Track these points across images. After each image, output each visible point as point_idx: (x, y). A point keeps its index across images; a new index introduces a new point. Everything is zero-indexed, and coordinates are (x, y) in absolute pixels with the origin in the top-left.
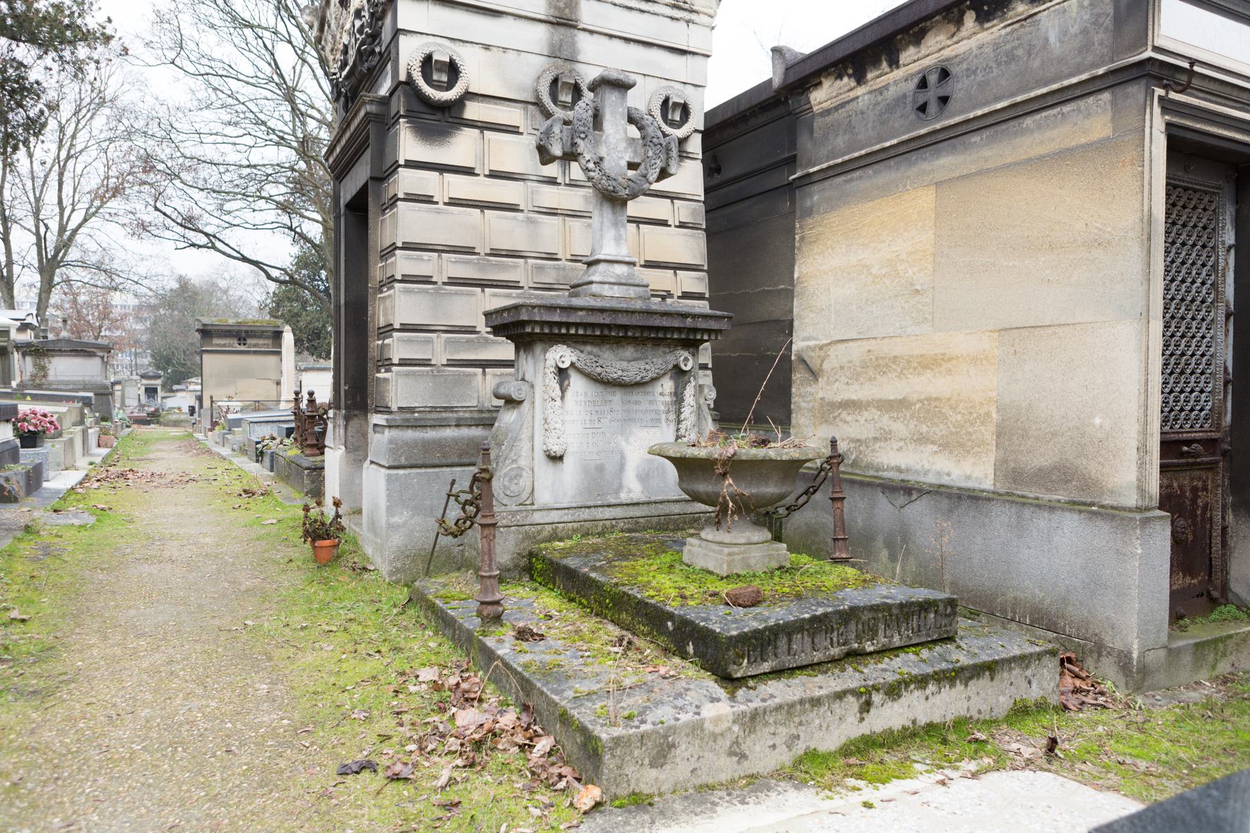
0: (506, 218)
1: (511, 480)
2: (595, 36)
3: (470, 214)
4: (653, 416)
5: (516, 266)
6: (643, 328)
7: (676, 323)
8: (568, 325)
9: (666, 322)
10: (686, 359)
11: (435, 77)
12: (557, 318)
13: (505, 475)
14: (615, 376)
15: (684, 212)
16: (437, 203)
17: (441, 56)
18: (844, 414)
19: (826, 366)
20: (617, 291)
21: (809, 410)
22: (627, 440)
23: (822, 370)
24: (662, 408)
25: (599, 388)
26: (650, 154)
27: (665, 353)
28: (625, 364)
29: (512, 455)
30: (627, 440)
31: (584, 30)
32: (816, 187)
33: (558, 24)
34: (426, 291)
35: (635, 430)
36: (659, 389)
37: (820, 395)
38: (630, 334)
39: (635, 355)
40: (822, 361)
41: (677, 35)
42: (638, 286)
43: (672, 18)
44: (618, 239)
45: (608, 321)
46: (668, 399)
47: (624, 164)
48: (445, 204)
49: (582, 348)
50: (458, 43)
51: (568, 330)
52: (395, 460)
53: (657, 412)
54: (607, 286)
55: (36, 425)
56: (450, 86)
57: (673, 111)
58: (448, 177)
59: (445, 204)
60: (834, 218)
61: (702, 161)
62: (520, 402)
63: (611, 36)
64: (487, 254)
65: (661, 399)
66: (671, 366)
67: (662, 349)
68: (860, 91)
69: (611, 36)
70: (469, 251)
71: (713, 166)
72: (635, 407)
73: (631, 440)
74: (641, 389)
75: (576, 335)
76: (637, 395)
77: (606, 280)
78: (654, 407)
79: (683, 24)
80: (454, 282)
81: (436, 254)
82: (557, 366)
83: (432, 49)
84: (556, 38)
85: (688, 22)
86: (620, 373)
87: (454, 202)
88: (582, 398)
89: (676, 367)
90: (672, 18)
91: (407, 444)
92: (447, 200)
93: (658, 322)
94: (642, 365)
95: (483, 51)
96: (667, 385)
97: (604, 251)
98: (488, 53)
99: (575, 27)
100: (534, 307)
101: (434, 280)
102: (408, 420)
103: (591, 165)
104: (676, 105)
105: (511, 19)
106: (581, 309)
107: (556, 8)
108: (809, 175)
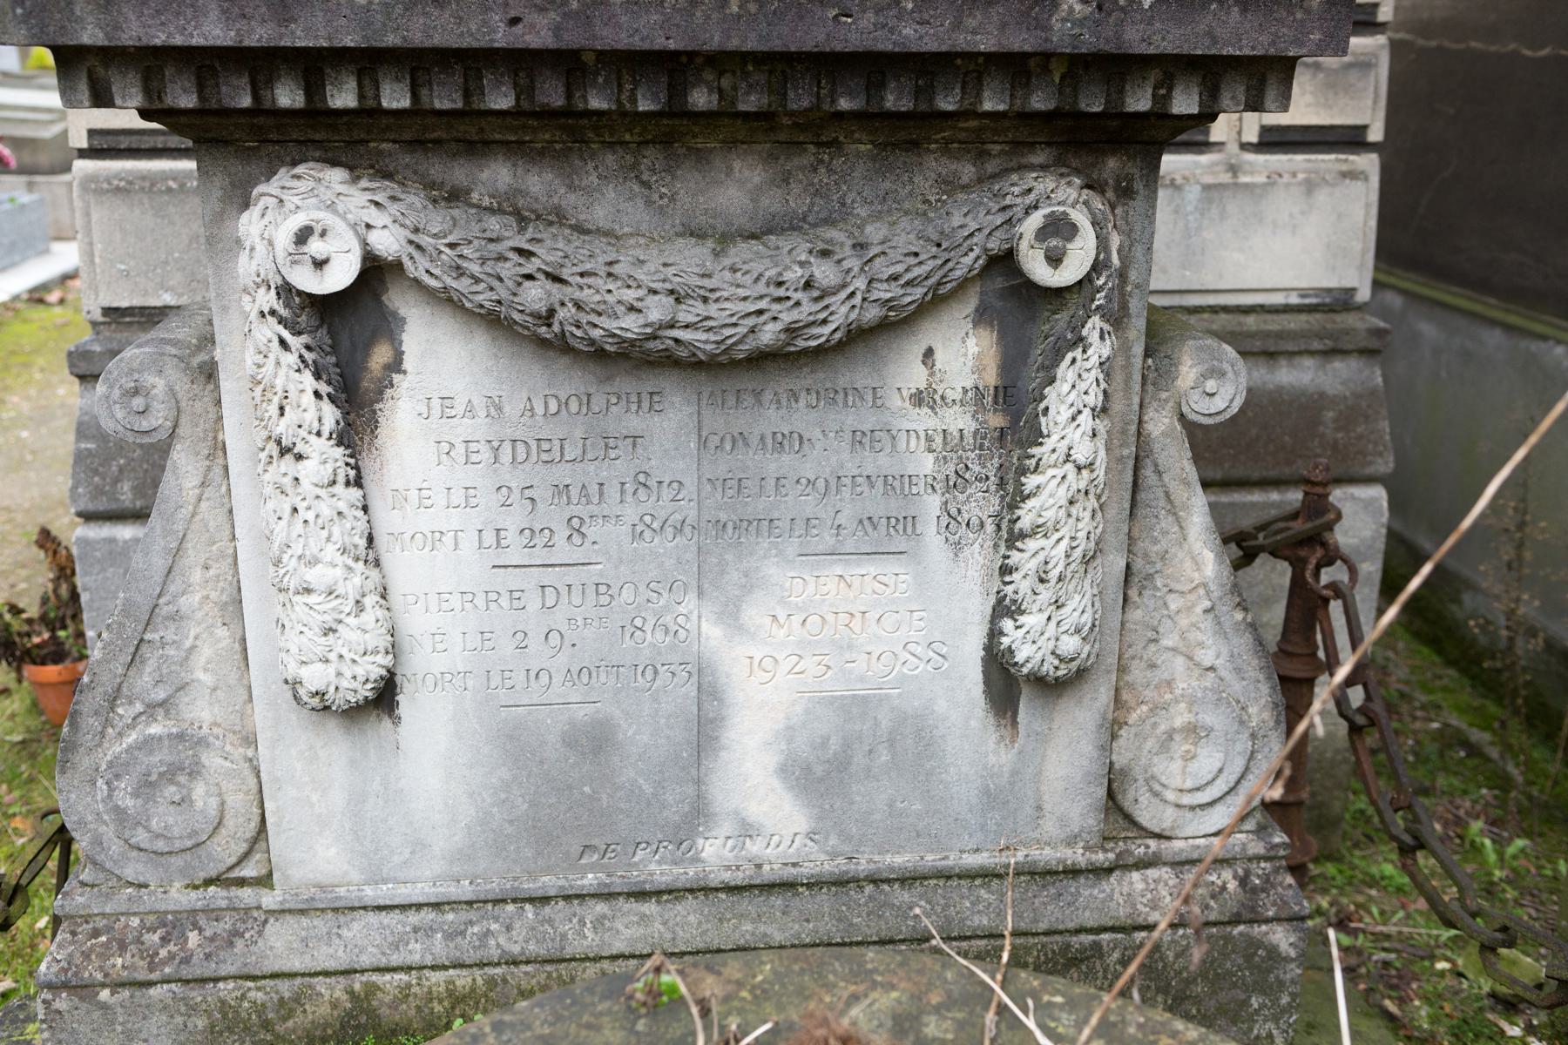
1: (147, 787)
4: (876, 503)
10: (1059, 229)
13: (117, 769)
14: (631, 325)
22: (730, 615)
25: (572, 382)
27: (950, 186)
28: (689, 260)
29: (144, 679)
30: (730, 615)
35: (772, 570)
38: (701, 99)
39: (772, 202)
46: (960, 421)
49: (459, 173)
51: (314, 89)
52: (98, 492)
53: (897, 484)
65: (923, 420)
66: (968, 262)
67: (935, 165)
72: (774, 465)
73: (754, 614)
74: (804, 379)
75: (369, 114)
76: (778, 411)
78: (879, 463)
82: (286, 290)
86: (657, 310)
88: (477, 428)
89: (1004, 262)
94: (793, 260)
96: (962, 352)
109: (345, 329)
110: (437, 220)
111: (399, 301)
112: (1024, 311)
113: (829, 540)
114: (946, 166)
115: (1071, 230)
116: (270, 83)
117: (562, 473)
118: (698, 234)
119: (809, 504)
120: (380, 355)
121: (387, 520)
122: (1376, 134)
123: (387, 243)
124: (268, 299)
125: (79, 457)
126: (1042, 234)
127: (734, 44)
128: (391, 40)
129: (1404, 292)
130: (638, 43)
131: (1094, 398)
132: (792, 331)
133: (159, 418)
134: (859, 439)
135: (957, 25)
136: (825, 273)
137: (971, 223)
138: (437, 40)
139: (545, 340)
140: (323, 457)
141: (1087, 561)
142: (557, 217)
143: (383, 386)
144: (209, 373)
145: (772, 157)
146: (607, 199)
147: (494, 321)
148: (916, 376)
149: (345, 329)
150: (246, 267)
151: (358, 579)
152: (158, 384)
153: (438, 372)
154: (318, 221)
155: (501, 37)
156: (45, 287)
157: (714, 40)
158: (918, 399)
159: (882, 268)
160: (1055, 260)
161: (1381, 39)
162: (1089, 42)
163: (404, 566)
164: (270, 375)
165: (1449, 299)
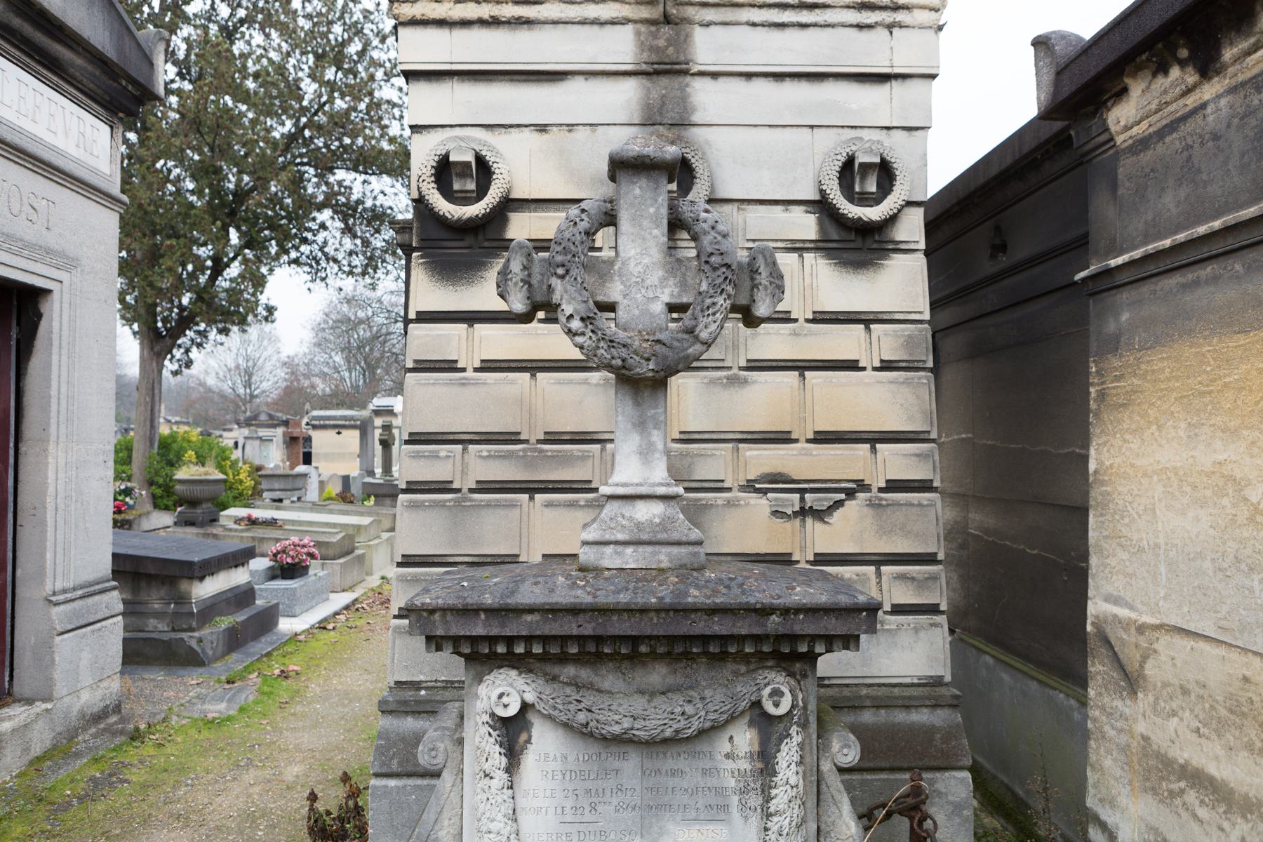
0: (571, 382)
2: (721, 80)
3: (512, 382)
5: (584, 457)
6: (672, 639)
7: (743, 627)
8: (510, 641)
9: (718, 627)
10: (777, 693)
11: (456, 187)
12: (479, 630)
14: (617, 729)
15: (887, 342)
16: (464, 370)
18: (1191, 797)
19: (1150, 670)
20: (631, 558)
21: (1125, 749)
23: (1144, 677)
24: (732, 783)
25: (594, 748)
26: (704, 287)
27: (737, 674)
28: (639, 704)
31: (702, 74)
32: (1124, 296)
33: (658, 73)
34: (441, 504)
35: (671, 826)
36: (726, 747)
37: (1141, 727)
39: (670, 680)
40: (1144, 659)
41: (873, 51)
42: (678, 543)
43: (860, 27)
44: (645, 453)
45: (588, 630)
46: (745, 765)
47: (658, 308)
48: (476, 370)
52: (383, 764)
53: (720, 791)
54: (609, 550)
55: (293, 558)
56: (482, 192)
58: (481, 329)
59: (476, 370)
61: (927, 253)
62: (437, 775)
63: (749, 76)
64: (539, 442)
65: (730, 765)
66: (744, 705)
68: (1209, 91)
69: (749, 76)
70: (511, 438)
71: (997, 241)
72: (671, 782)
74: (684, 748)
76: (673, 761)
77: (608, 537)
79: (882, 33)
80: (485, 487)
81: (460, 447)
82: (493, 715)
83: (450, 146)
84: (655, 95)
85: (890, 27)
86: (626, 724)
87: (489, 366)
88: (557, 766)
89: (757, 704)
90: (860, 27)
91: (403, 739)
92: (477, 365)
93: (700, 626)
94: (677, 704)
95: (536, 135)
96: (744, 738)
97: (615, 478)
98: (545, 136)
99: (686, 72)
100: (432, 612)
101: (455, 486)
102: (405, 703)
103: (576, 324)
104: (866, 167)
105: (581, 79)
106: (531, 610)
107: (652, 49)
108: (1109, 272)
109: (512, 732)
110: (548, 689)
111: (531, 717)
113: (693, 814)
114: (735, 667)
115: (782, 694)
116: (495, 644)
117: (589, 785)
118: (642, 692)
119: (685, 799)
120: (523, 737)
121: (521, 802)
122: (943, 607)
123: (530, 697)
124: (486, 718)
125: (378, 748)
126: (771, 695)
127: (655, 633)
128: (538, 633)
129: (993, 657)
130: (621, 633)
131: (796, 758)
132: (677, 731)
133: (440, 760)
134: (705, 772)
135: (734, 625)
136: (689, 709)
137: (744, 690)
138: (553, 633)
139: (584, 733)
140: (500, 777)
141: (798, 827)
142: (590, 687)
143: (524, 748)
144: (460, 742)
145: (670, 663)
146: (609, 679)
147: (567, 726)
148: (726, 747)
149: (512, 732)
150: (481, 705)
151: (508, 828)
152: (441, 746)
153: (544, 743)
154: (504, 690)
155: (575, 632)
156: (325, 620)
158: (728, 756)
159: (711, 707)
160: (777, 705)
161: (941, 567)
162: (781, 631)
163: (526, 821)
164: (482, 745)
165: (1013, 663)
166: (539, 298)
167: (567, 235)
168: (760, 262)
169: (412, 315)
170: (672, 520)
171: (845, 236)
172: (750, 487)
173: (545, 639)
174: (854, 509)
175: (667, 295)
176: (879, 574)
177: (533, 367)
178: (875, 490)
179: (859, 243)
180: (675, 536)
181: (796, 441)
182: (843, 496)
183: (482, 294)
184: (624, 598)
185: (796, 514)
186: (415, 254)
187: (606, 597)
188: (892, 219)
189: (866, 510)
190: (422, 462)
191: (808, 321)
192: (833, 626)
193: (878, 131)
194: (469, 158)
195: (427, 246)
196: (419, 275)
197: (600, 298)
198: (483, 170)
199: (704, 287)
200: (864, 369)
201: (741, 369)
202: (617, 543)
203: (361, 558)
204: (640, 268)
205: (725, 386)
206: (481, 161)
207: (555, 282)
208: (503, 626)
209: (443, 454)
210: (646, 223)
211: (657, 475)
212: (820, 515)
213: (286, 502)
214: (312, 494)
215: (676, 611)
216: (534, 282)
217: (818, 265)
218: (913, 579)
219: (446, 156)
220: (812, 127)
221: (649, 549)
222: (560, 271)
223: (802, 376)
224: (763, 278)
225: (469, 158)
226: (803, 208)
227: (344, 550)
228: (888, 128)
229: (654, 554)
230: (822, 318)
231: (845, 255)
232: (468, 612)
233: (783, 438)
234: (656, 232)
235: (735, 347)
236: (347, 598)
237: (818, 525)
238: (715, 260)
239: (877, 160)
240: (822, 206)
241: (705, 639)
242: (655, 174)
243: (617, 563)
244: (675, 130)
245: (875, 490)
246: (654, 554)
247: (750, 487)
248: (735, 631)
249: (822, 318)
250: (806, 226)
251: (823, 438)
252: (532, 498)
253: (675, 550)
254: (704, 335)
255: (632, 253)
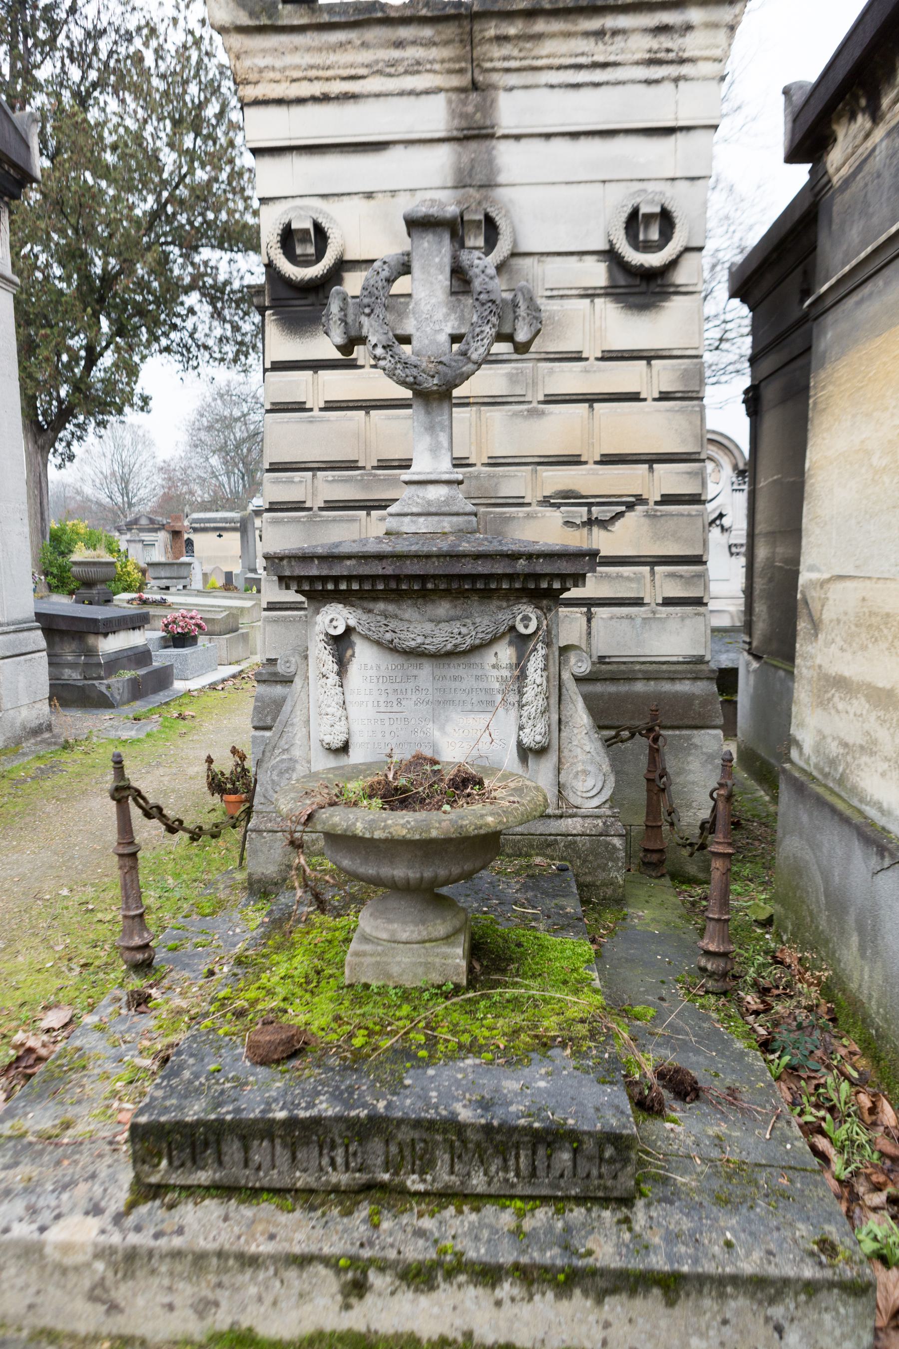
0: (398, 417)
1: (281, 774)
2: (524, 141)
3: (351, 419)
4: (483, 697)
6: (450, 577)
7: (499, 568)
8: (336, 579)
9: (482, 568)
10: (526, 619)
11: (299, 251)
12: (314, 572)
13: (274, 768)
14: (413, 644)
16: (311, 410)
17: (302, 223)
20: (423, 525)
22: (442, 729)
24: (497, 685)
25: (399, 660)
26: (475, 319)
27: (500, 608)
28: (428, 627)
29: (283, 742)
30: (442, 729)
31: (506, 137)
32: (830, 318)
33: (467, 138)
34: (297, 520)
35: (454, 716)
36: (492, 660)
38: (430, 586)
39: (452, 613)
41: (659, 106)
42: (457, 514)
43: (649, 82)
45: (389, 571)
46: (506, 673)
47: (443, 338)
48: (321, 409)
49: (371, 605)
50: (331, 199)
51: (336, 585)
52: (260, 720)
54: (407, 519)
56: (320, 254)
57: (647, 228)
59: (321, 409)
60: (822, 375)
63: (548, 136)
64: (374, 468)
65: (495, 673)
67: (496, 603)
68: (880, 133)
69: (548, 136)
70: (351, 465)
72: (454, 685)
73: (449, 728)
74: (462, 660)
75: (349, 591)
76: (456, 669)
78: (483, 685)
79: (668, 86)
80: (331, 506)
82: (327, 634)
83: (292, 215)
84: (465, 159)
85: (676, 80)
86: (420, 640)
88: (373, 673)
89: (513, 628)
90: (649, 82)
91: (275, 702)
92: (322, 405)
93: (468, 568)
94: (456, 627)
98: (372, 202)
99: (491, 136)
100: (281, 559)
101: (307, 505)
104: (649, 217)
105: (400, 149)
106: (349, 557)
108: (821, 297)
109: (341, 644)
110: (365, 617)
111: (355, 638)
112: (522, 642)
113: (470, 707)
114: (499, 603)
115: (530, 619)
117: (396, 686)
118: (432, 621)
119: (464, 697)
120: (349, 652)
121: (348, 698)
123: (352, 623)
124: (322, 637)
125: (255, 708)
126: (522, 620)
131: (541, 665)
132: (456, 646)
133: (292, 669)
134: (477, 678)
136: (464, 630)
137: (504, 617)
139: (392, 648)
140: (333, 678)
141: (543, 713)
142: (396, 616)
143: (350, 660)
144: (306, 657)
146: (408, 612)
147: (378, 643)
148: (492, 660)
149: (341, 644)
150: (318, 628)
151: (340, 712)
152: (293, 660)
153: (364, 656)
154: (336, 617)
155: (380, 572)
157: (432, 572)
158: (494, 666)
159: (480, 629)
160: (526, 627)
162: (527, 571)
163: (352, 710)
164: (321, 656)
166: (353, 333)
167: (372, 282)
168: (520, 298)
169: (268, 365)
170: (453, 498)
171: (631, 281)
172: (546, 502)
173: (361, 578)
174: (632, 518)
175: (450, 327)
176: (653, 573)
177: (367, 406)
178: (651, 503)
179: (643, 288)
180: (455, 509)
181: (586, 463)
182: (623, 508)
183: (324, 347)
184: (414, 548)
185: (584, 524)
186: (268, 313)
187: (402, 547)
188: (673, 264)
189: (643, 520)
190: (281, 486)
191: (597, 359)
192: (565, 567)
193: (663, 183)
194: (309, 225)
195: (278, 305)
196: (272, 330)
197: (399, 332)
198: (320, 234)
199: (475, 319)
200: (645, 400)
201: (540, 402)
202: (412, 514)
203: (245, 637)
204: (429, 307)
205: (525, 417)
206: (318, 228)
207: (364, 320)
208: (331, 568)
209: (297, 479)
210: (433, 270)
211: (443, 467)
212: (604, 524)
213: (172, 590)
214: (197, 583)
215: (451, 556)
216: (350, 320)
217: (607, 309)
218: (681, 576)
219: (289, 225)
220: (604, 182)
221: (436, 518)
222: (367, 310)
223: (591, 407)
224: (522, 311)
225: (309, 225)
226: (595, 258)
227: (230, 626)
228: (673, 179)
229: (439, 522)
230: (609, 356)
231: (631, 299)
232: (305, 558)
233: (574, 461)
234: (441, 277)
235: (534, 383)
236: (234, 669)
237: (603, 533)
238: (483, 297)
239: (657, 210)
240: (611, 255)
241: (473, 578)
242: (439, 230)
243: (413, 529)
244: (483, 191)
245: (651, 503)
246: (439, 522)
247: (546, 502)
248: (494, 571)
249: (609, 356)
250: (597, 274)
251: (608, 460)
252: (368, 514)
253: (455, 519)
254: (475, 356)
255: (423, 295)
